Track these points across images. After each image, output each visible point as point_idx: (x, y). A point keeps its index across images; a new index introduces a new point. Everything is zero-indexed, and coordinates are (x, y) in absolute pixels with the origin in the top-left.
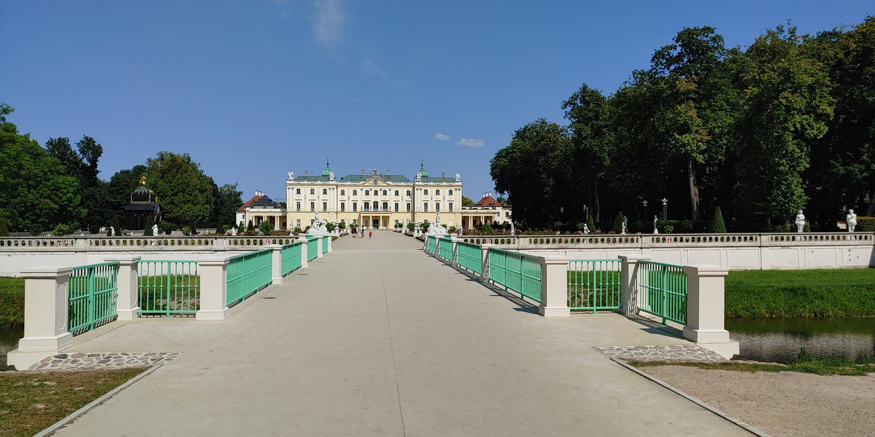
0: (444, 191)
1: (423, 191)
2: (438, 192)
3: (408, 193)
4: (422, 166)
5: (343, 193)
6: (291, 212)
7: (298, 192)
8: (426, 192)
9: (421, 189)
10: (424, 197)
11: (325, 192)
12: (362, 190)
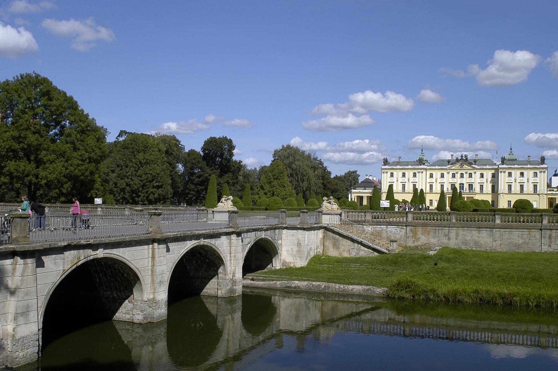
0: (529, 174)
1: (507, 174)
2: (522, 174)
4: (511, 150)
5: (431, 176)
7: (392, 175)
8: (510, 174)
9: (504, 172)
10: (508, 179)
11: (415, 175)
12: (448, 173)
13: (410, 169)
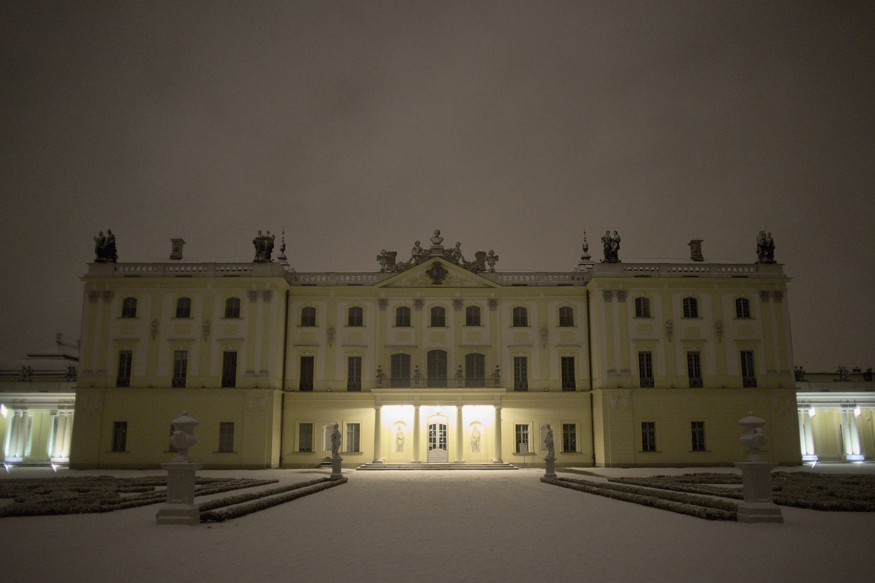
2: (691, 308)
4: (586, 250)
5: (309, 319)
8: (642, 309)
9: (622, 296)
11: (233, 311)
12: (383, 303)
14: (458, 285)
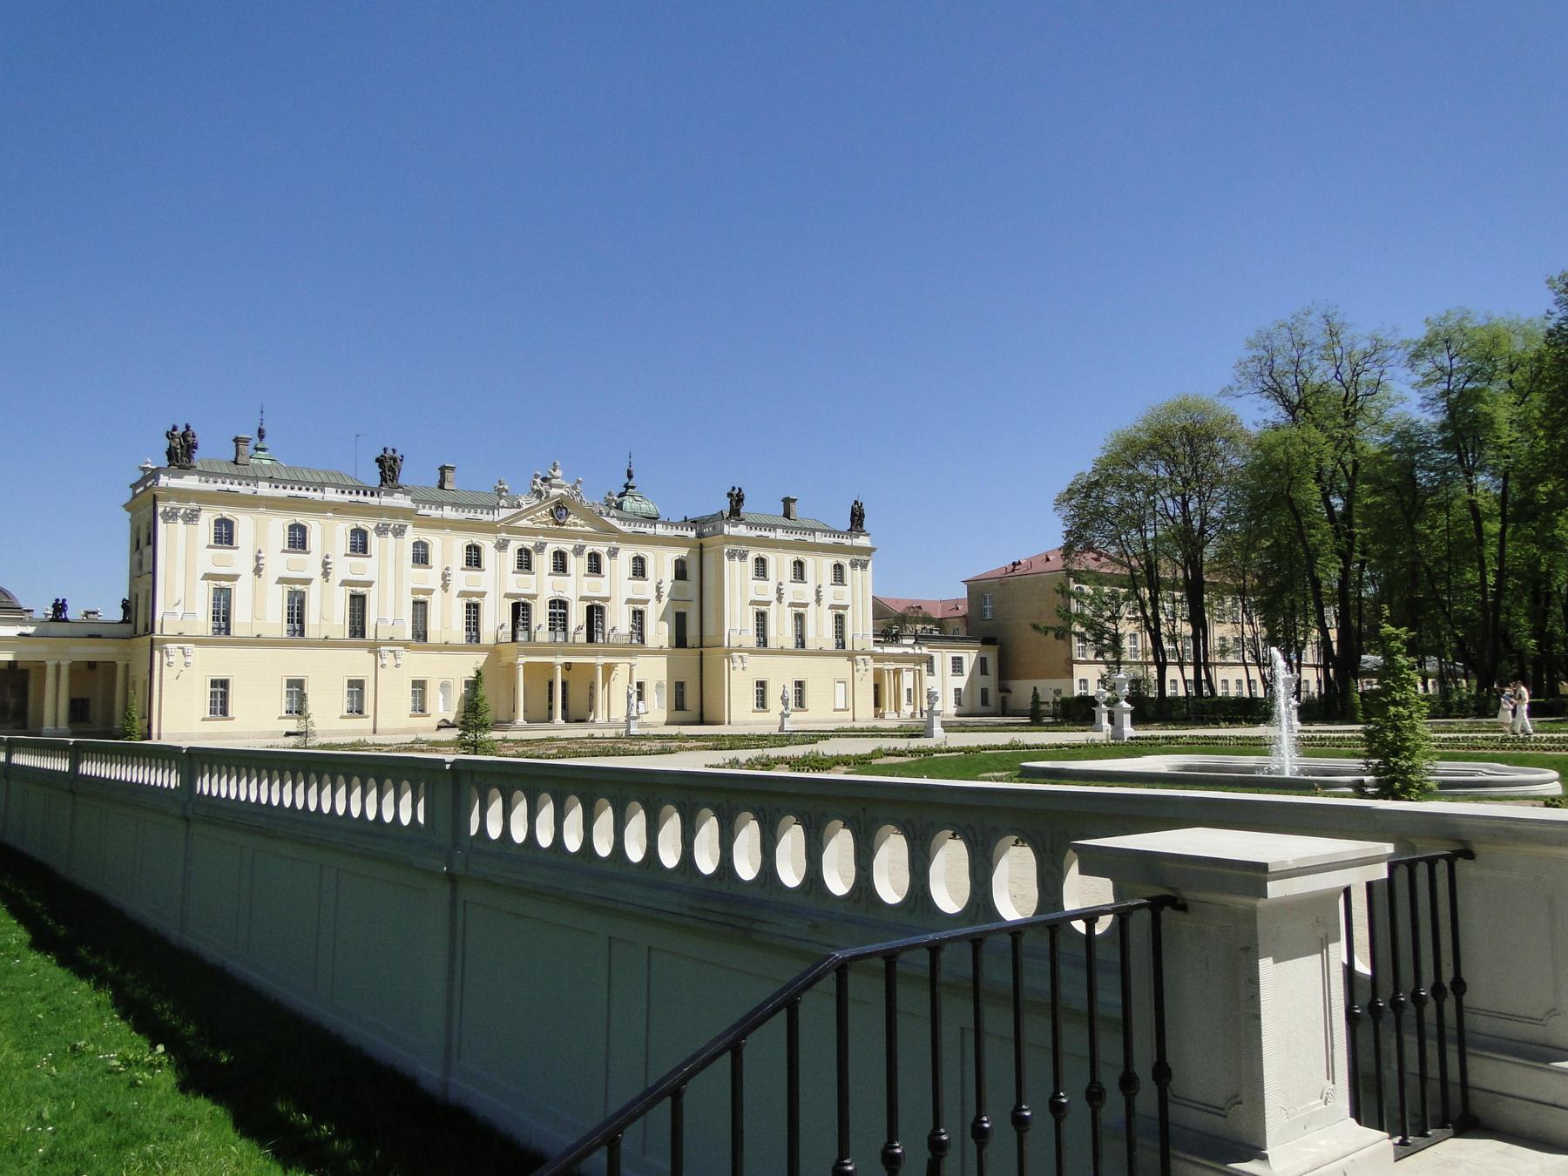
1: (750, 562)
3: (681, 572)
4: (630, 476)
5: (421, 556)
6: (180, 638)
7: (225, 534)
8: (761, 566)
9: (743, 556)
11: (359, 544)
12: (502, 546)
13: (338, 509)
14: (579, 528)
